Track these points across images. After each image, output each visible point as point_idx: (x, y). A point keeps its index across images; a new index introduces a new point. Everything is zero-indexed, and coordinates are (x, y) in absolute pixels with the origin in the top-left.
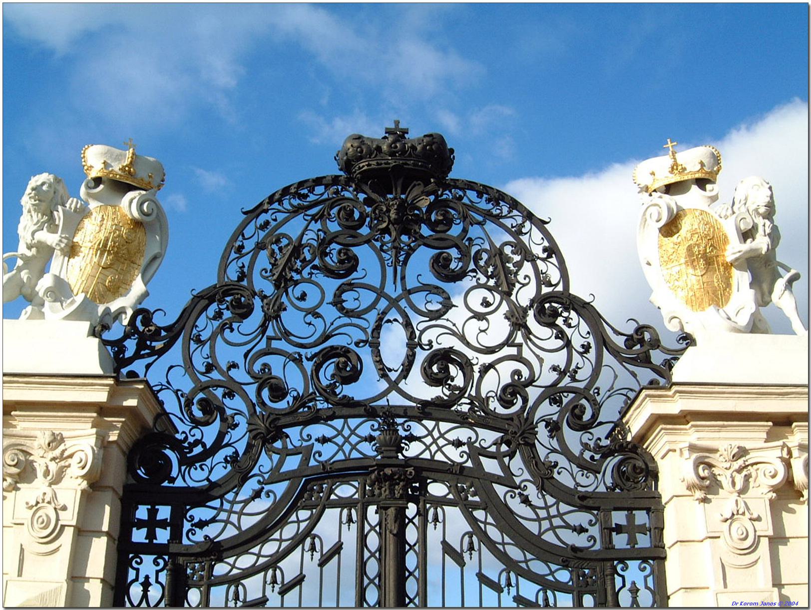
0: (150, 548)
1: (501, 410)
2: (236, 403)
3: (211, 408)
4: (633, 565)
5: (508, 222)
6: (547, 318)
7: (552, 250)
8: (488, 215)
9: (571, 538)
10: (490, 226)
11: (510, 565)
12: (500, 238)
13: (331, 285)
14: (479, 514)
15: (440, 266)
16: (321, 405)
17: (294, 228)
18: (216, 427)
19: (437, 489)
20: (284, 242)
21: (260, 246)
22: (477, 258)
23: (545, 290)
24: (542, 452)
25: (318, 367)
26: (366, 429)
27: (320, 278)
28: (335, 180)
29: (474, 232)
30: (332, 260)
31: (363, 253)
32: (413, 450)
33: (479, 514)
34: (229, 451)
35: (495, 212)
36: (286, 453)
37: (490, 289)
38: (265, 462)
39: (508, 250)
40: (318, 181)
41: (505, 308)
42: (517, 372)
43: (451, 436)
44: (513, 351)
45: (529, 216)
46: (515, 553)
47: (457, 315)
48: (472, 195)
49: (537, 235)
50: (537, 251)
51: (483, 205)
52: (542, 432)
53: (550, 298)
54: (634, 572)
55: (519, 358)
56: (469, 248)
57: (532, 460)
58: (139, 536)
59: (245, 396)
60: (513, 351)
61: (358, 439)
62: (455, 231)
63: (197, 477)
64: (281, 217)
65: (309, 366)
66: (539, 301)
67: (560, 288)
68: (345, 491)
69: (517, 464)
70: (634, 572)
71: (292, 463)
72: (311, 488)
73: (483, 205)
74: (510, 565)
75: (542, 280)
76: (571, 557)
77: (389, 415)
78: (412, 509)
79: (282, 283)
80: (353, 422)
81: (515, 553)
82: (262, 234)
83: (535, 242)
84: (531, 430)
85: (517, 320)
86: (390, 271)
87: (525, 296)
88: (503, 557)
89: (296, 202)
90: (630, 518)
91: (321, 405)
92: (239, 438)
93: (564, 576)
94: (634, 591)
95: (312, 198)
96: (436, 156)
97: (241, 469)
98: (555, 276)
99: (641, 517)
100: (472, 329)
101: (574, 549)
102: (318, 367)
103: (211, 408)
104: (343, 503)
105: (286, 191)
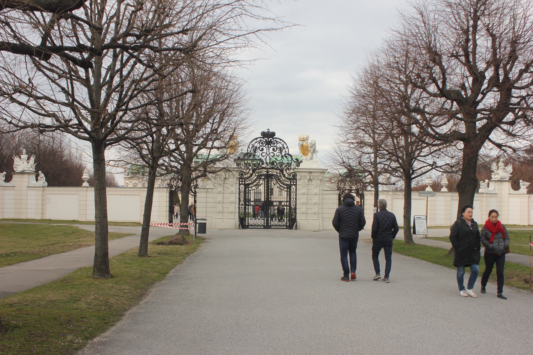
0: (242, 184)
2: (250, 167)
3: (248, 168)
6: (286, 157)
7: (287, 147)
12: (281, 146)
13: (261, 152)
15: (273, 149)
17: (256, 145)
18: (248, 170)
26: (265, 170)
31: (264, 148)
38: (254, 175)
47: (275, 157)
51: (279, 141)
57: (283, 174)
58: (241, 183)
61: (264, 172)
63: (247, 176)
66: (285, 155)
68: (263, 177)
71: (257, 174)
72: (259, 177)
73: (279, 141)
77: (268, 168)
79: (255, 152)
83: (285, 146)
85: (282, 157)
87: (283, 154)
92: (251, 172)
96: (273, 134)
97: (251, 175)
98: (287, 151)
100: (277, 158)
103: (248, 168)
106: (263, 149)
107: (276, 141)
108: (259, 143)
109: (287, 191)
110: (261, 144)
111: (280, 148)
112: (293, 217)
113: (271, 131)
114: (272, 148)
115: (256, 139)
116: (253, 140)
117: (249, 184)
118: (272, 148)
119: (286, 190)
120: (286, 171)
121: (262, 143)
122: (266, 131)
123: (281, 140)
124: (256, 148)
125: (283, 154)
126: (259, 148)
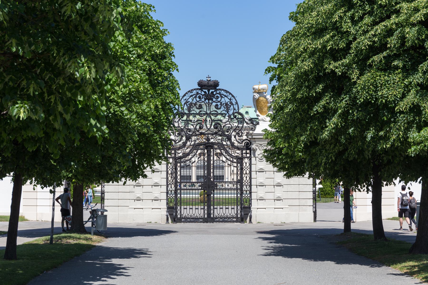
1: (226, 133)
4: (246, 159)
5: (229, 97)
7: (237, 103)
8: (225, 96)
9: (236, 154)
10: (225, 98)
11: (227, 159)
12: (227, 100)
14: (222, 151)
15: (216, 106)
16: (197, 133)
19: (216, 147)
20: (189, 103)
21: (184, 104)
22: (223, 104)
23: (235, 111)
24: (233, 141)
25: (196, 127)
27: (196, 110)
28: (197, 89)
29: (223, 99)
30: (197, 106)
32: (212, 140)
33: (222, 151)
34: (183, 141)
35: (227, 95)
36: (192, 141)
37: (226, 111)
38: (188, 143)
39: (229, 103)
40: (194, 90)
41: (228, 115)
42: (229, 127)
43: (218, 138)
44: (228, 123)
45: (233, 96)
46: (228, 157)
48: (222, 91)
49: (234, 99)
50: (234, 103)
51: (225, 94)
52: (233, 137)
53: (236, 113)
54: (246, 160)
55: (230, 124)
56: (222, 103)
59: (184, 131)
60: (229, 123)
62: (219, 100)
64: (188, 97)
65: (195, 126)
66: (233, 114)
67: (237, 111)
68: (202, 147)
69: (229, 143)
70: (246, 160)
73: (225, 94)
74: (227, 159)
75: (234, 109)
76: (237, 157)
78: (212, 150)
80: (202, 136)
81: (228, 157)
82: (185, 101)
83: (234, 101)
84: (231, 137)
86: (208, 107)
87: (231, 112)
88: (226, 158)
89: (191, 94)
90: (246, 152)
91: (197, 133)
92: (184, 138)
93: (235, 161)
94: (246, 163)
95: (193, 93)
98: (237, 108)
99: (248, 151)
101: (236, 157)
102: (196, 127)
104: (201, 149)
105: (189, 91)
106: (200, 107)
107: (220, 94)
108: (196, 97)
109: (237, 167)
110: (198, 99)
111: (226, 104)
112: (246, 205)
113: (212, 79)
114: (214, 104)
115: (191, 91)
116: (186, 93)
117: (180, 158)
118: (214, 104)
119: (235, 165)
120: (235, 137)
121: (200, 98)
122: (205, 79)
123: (227, 92)
124: (191, 104)
125: (231, 112)
126: (195, 104)
